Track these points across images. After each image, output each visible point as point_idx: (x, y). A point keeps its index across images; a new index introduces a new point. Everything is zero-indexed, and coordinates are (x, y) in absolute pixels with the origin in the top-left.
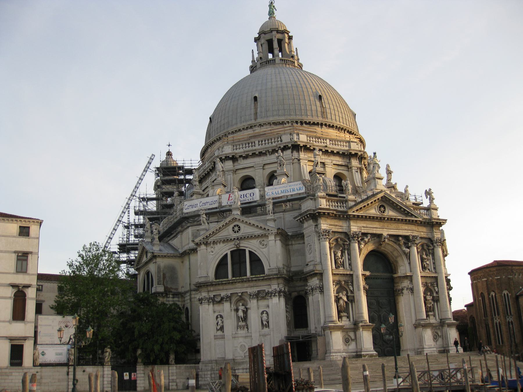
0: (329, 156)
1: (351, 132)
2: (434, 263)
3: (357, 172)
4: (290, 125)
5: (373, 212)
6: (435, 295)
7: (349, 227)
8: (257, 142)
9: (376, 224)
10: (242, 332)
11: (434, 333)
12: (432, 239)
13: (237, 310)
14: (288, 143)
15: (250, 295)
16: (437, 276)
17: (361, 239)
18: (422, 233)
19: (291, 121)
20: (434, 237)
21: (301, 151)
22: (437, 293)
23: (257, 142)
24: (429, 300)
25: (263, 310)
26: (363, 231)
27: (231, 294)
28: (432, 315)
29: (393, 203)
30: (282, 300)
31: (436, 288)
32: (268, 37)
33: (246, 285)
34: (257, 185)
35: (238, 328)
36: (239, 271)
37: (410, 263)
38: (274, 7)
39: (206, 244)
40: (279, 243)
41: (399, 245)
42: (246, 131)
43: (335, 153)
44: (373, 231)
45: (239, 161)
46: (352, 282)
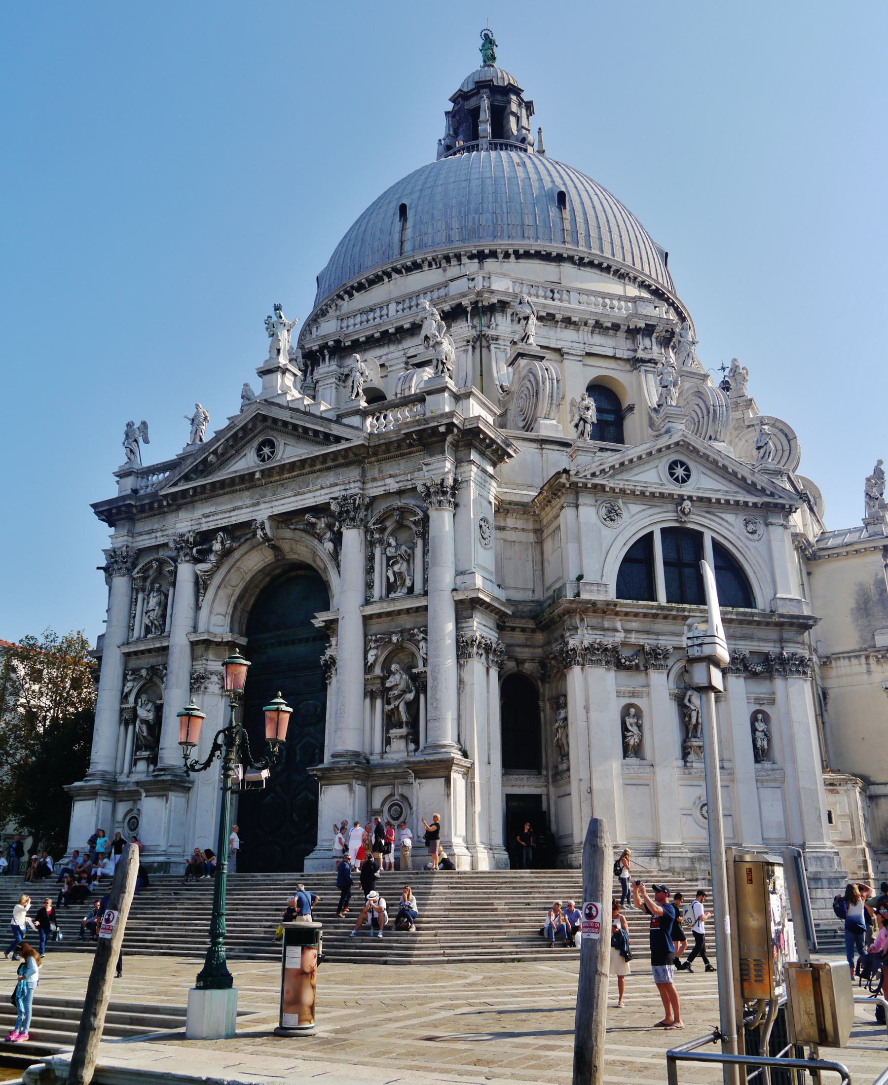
0: (399, 342)
1: (483, 251)
3: (466, 351)
11: (397, 797)
16: (424, 603)
17: (198, 551)
18: (389, 481)
19: (333, 300)
21: (324, 359)
22: (425, 661)
24: (391, 689)
26: (205, 528)
28: (401, 737)
29: (285, 424)
41: (320, 539)
43: (408, 329)
44: (230, 519)
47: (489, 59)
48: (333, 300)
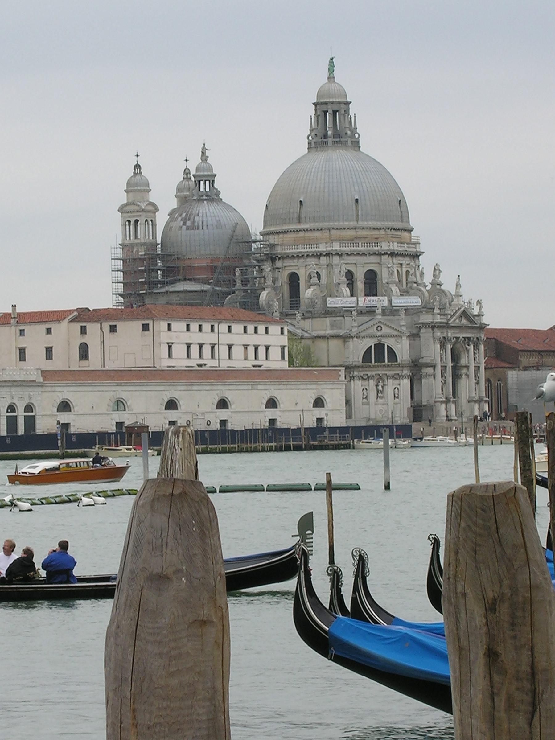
2: (479, 356)
4: (384, 230)
6: (477, 378)
7: (447, 332)
8: (360, 244)
10: (380, 401)
12: (479, 338)
13: (377, 386)
14: (388, 250)
15: (388, 377)
20: (481, 337)
22: (478, 378)
23: (360, 244)
25: (395, 387)
27: (376, 374)
30: (409, 381)
31: (478, 374)
33: (385, 369)
34: (358, 280)
35: (377, 398)
37: (468, 357)
38: (333, 63)
40: (408, 341)
42: (349, 230)
45: (343, 257)
46: (446, 371)
47: (331, 70)
48: (386, 228)
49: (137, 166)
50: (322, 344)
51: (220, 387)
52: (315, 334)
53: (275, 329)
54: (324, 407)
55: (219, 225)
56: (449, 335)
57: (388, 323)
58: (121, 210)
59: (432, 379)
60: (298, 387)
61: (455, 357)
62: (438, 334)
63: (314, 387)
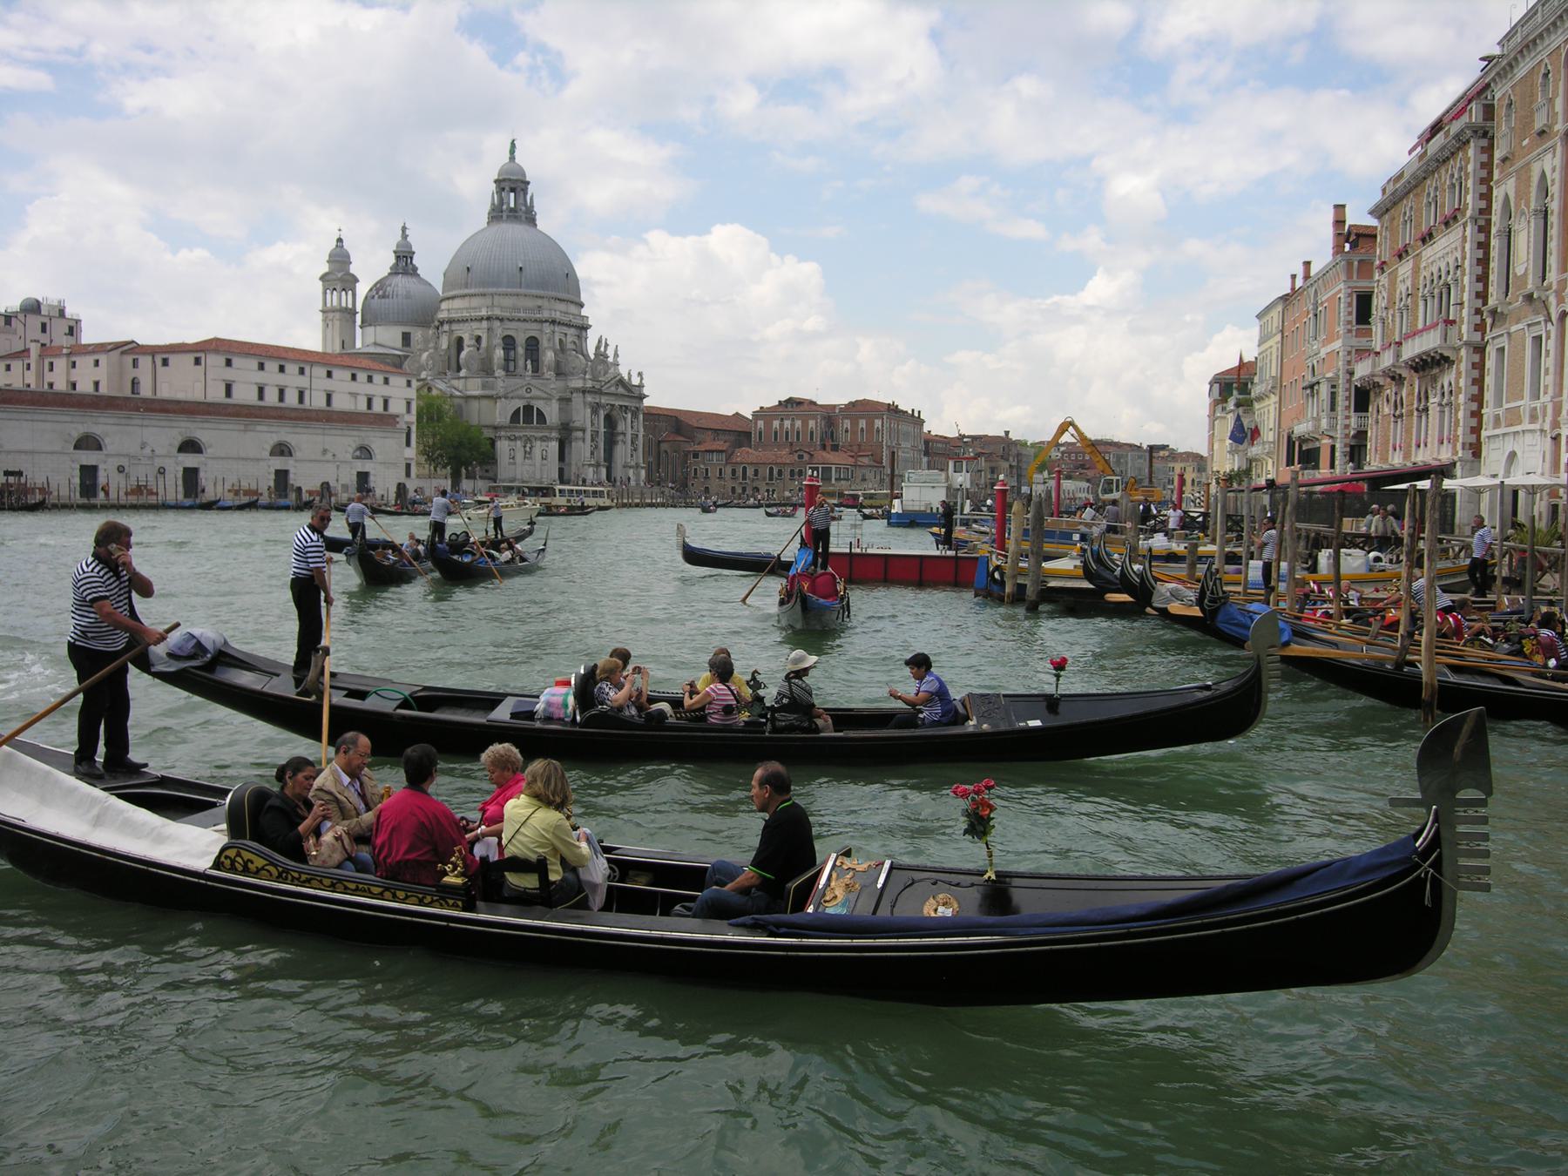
5: (613, 389)
9: (613, 398)
13: (525, 447)
32: (513, 186)
36: (528, 420)
39: (506, 398)
49: (340, 240)
50: (475, 404)
51: (183, 424)
52: (469, 393)
53: (398, 381)
54: (371, 458)
55: (408, 296)
56: (603, 401)
57: (539, 386)
58: (323, 278)
59: (581, 443)
60: (326, 432)
61: (610, 422)
62: (589, 398)
63: (355, 433)
